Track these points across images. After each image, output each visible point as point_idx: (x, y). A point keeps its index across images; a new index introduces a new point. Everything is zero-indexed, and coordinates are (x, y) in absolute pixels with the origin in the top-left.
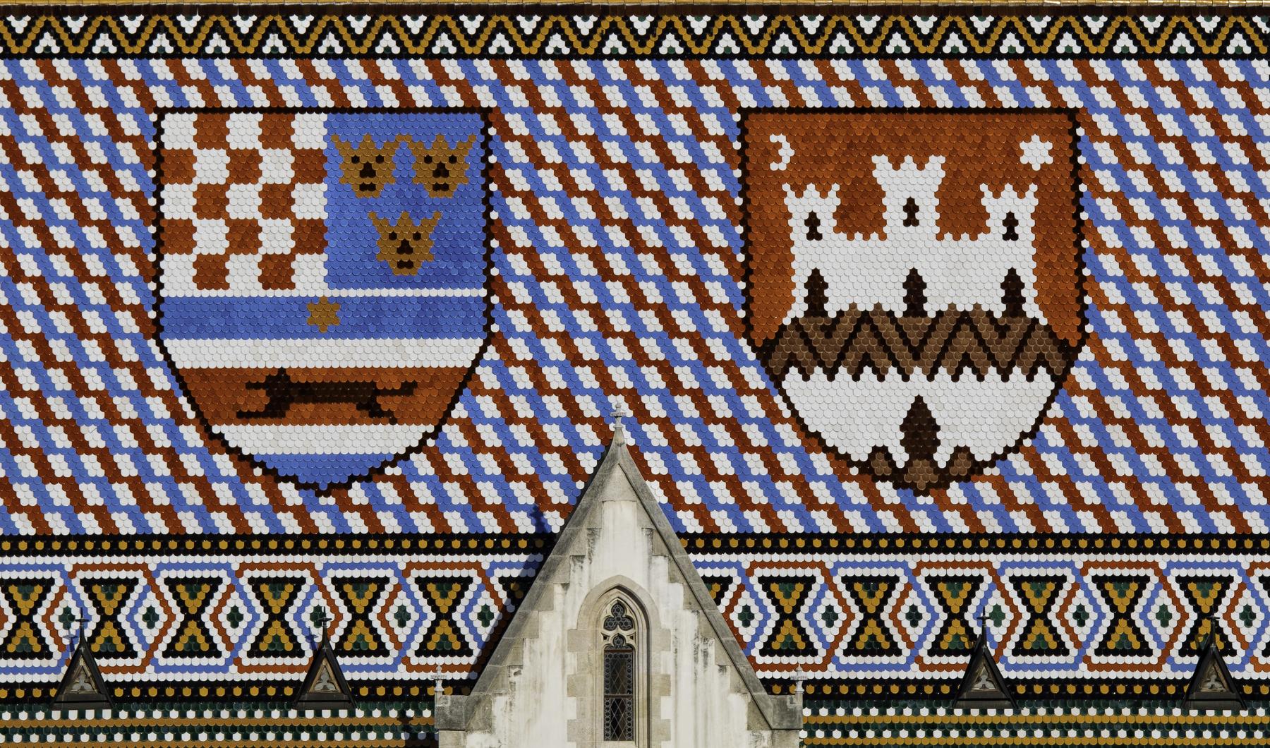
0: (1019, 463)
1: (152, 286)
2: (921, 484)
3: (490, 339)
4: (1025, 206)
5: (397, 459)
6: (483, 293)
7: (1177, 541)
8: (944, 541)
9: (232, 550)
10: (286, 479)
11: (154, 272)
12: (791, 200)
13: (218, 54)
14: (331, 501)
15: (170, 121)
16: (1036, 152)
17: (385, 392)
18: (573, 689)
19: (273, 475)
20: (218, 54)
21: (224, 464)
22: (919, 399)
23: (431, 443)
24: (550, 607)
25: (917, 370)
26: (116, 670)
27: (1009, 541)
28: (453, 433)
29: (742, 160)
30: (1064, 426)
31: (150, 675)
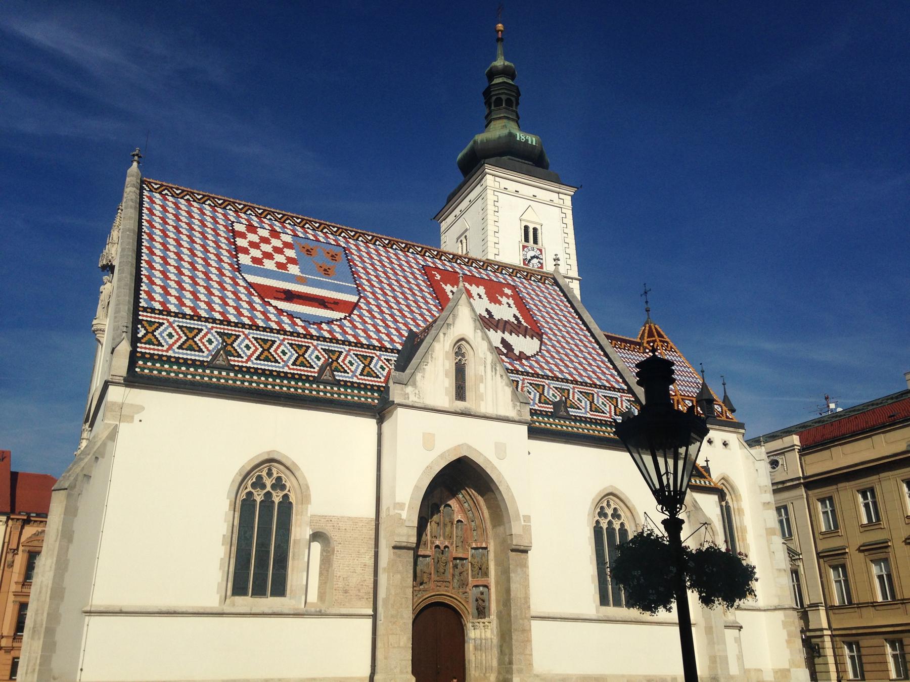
0: (539, 357)
1: (235, 260)
2: (514, 358)
3: (361, 297)
4: (511, 302)
5: (337, 320)
6: (356, 286)
7: (596, 386)
8: (528, 374)
9: (278, 332)
10: (297, 318)
11: (237, 257)
12: (443, 286)
13: (250, 214)
14: (315, 327)
15: (235, 224)
16: (508, 291)
17: (328, 302)
18: (447, 375)
19: (291, 316)
20: (250, 214)
21: (271, 309)
22: (503, 338)
23: (348, 318)
24: (439, 341)
25: (499, 331)
26: (234, 361)
27: (548, 377)
28: (355, 317)
29: (426, 274)
30: (548, 351)
31: (249, 364)
